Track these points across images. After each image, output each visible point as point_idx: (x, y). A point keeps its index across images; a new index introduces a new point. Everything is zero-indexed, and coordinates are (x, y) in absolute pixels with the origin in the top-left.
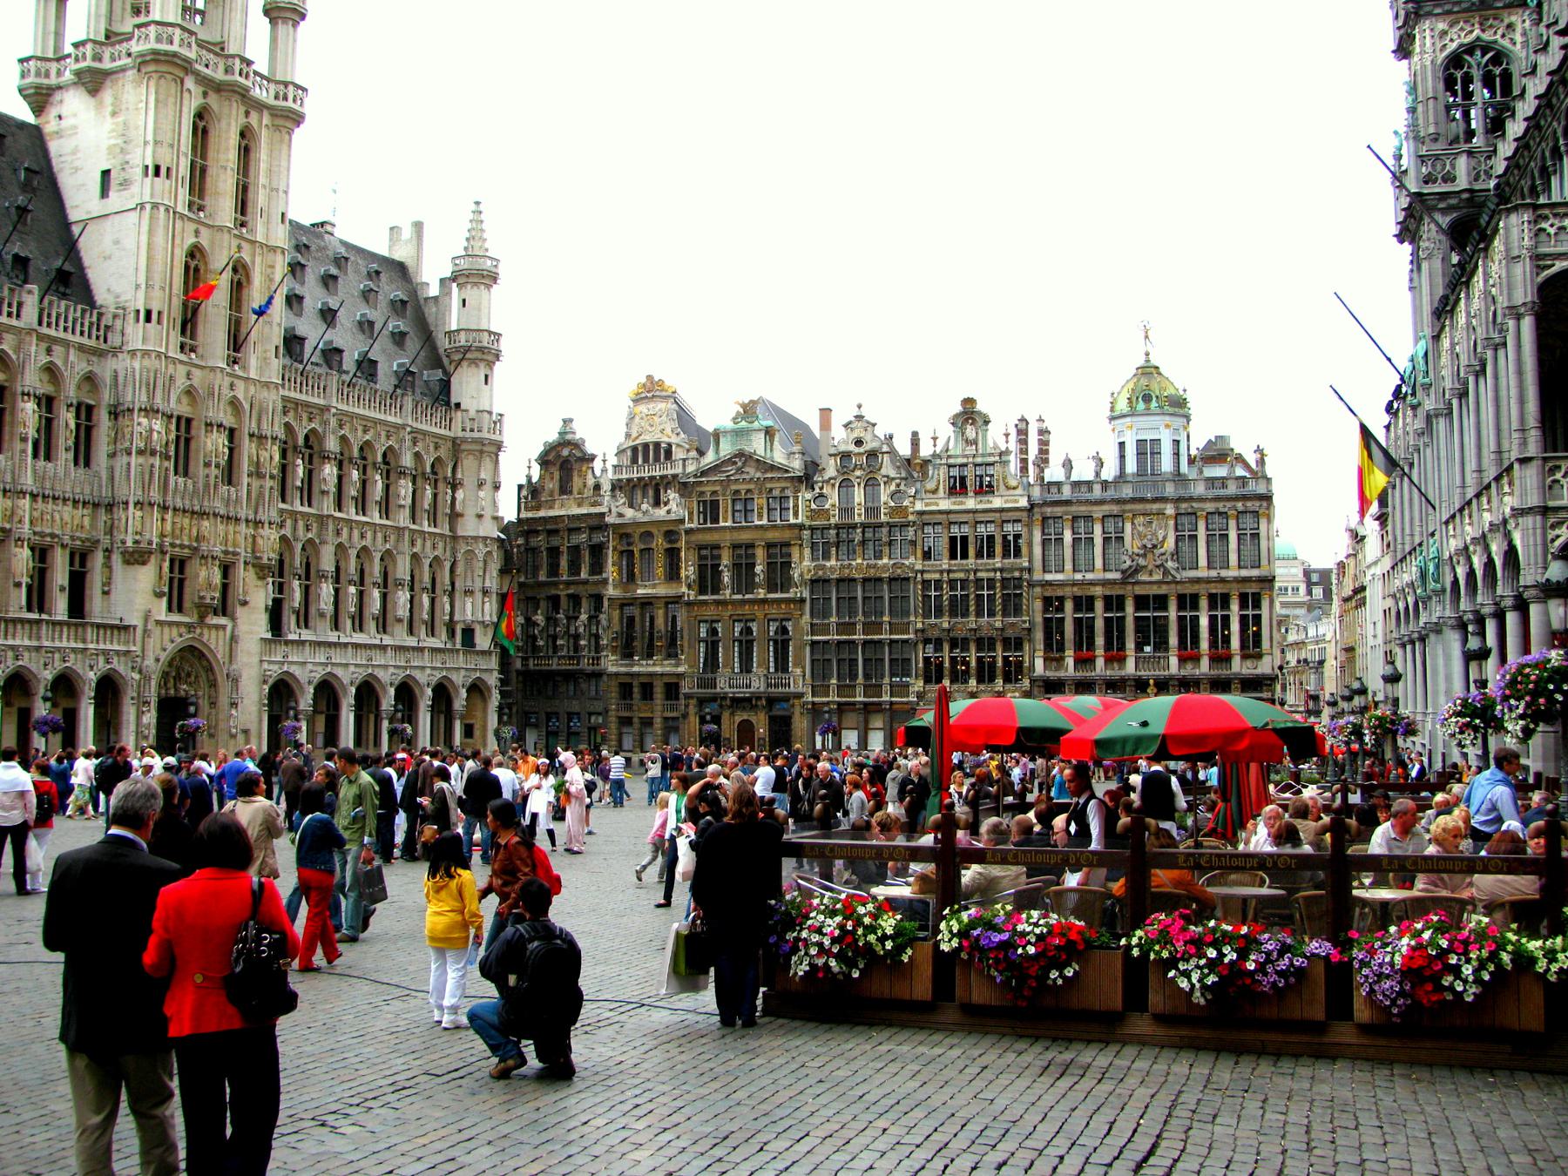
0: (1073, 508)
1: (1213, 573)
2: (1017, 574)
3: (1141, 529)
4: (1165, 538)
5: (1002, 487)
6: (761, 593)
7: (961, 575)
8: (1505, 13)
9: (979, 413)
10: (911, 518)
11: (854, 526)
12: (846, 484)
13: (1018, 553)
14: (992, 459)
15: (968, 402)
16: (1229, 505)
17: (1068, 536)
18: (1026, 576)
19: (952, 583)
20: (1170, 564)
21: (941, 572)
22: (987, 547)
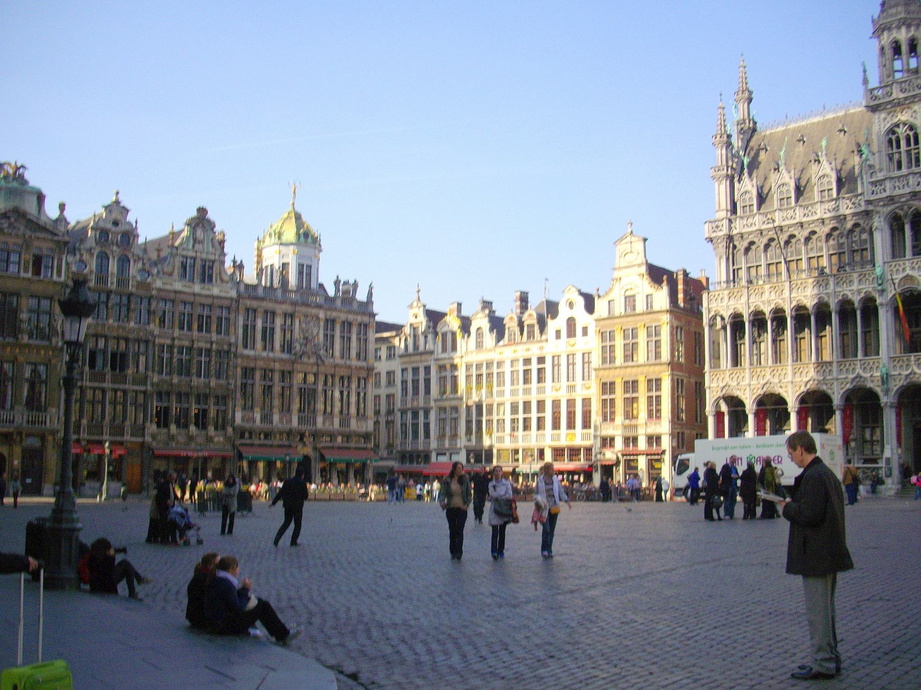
0: (264, 304)
1: (342, 362)
2: (226, 347)
3: (304, 325)
4: (318, 333)
5: (219, 281)
6: (25, 339)
7: (186, 343)
8: (911, 105)
9: (209, 221)
10: (154, 293)
11: (109, 293)
12: (103, 258)
13: (228, 333)
14: (212, 257)
15: (202, 211)
16: (355, 317)
17: (259, 324)
18: (233, 349)
19: (181, 348)
20: (322, 352)
21: (173, 339)
22: (204, 324)
